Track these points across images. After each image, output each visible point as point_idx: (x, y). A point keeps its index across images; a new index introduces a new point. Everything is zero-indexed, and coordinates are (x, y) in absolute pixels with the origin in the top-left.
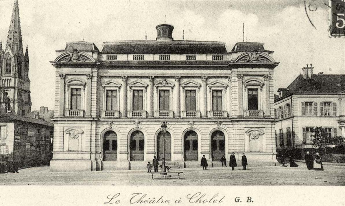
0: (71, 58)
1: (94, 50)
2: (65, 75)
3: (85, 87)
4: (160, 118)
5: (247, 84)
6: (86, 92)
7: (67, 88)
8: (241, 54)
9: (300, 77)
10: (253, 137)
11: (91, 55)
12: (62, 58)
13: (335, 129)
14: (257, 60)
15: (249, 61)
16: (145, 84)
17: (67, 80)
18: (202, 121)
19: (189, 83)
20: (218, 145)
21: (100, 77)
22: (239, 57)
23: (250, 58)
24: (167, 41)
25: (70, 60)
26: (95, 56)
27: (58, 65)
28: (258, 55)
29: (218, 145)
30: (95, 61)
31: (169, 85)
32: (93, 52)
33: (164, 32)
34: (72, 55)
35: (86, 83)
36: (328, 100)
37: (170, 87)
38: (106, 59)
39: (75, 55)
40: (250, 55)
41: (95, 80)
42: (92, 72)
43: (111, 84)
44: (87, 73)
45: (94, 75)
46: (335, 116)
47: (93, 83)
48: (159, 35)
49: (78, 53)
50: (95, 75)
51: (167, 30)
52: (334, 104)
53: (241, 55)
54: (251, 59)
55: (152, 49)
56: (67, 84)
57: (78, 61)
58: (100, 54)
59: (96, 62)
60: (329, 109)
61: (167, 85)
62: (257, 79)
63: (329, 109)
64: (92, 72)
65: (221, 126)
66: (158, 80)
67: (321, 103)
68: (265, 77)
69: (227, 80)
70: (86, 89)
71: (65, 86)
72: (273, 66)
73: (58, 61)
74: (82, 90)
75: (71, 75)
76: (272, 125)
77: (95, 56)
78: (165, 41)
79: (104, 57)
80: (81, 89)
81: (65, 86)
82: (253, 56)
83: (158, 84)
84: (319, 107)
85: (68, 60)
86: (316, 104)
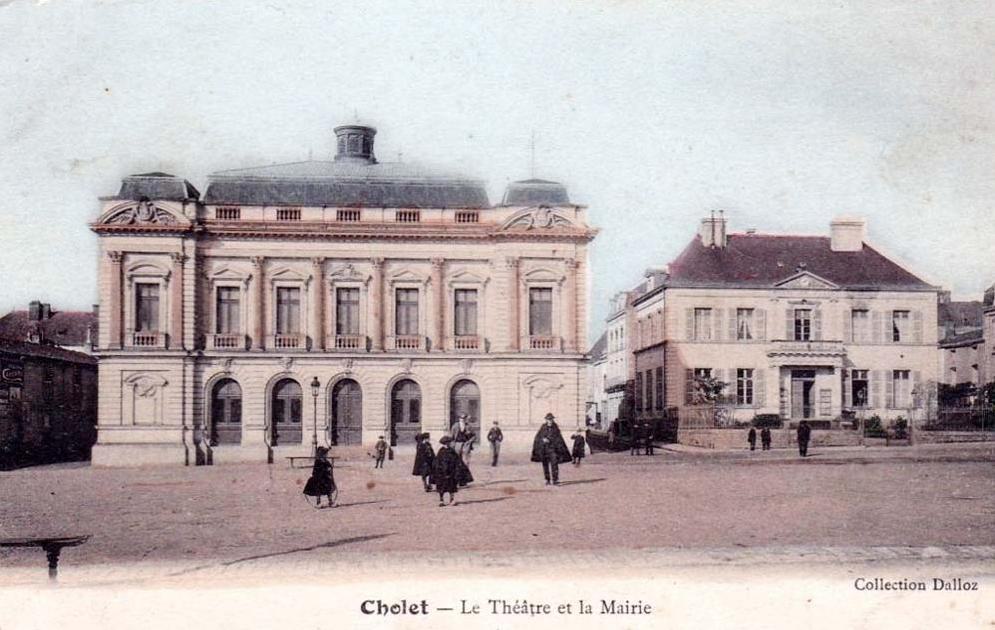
0: (135, 216)
1: (186, 196)
2: (120, 253)
3: (167, 280)
4: (336, 352)
5: (527, 277)
6: (170, 291)
7: (127, 282)
8: (514, 212)
9: (697, 242)
10: (537, 394)
11: (181, 211)
12: (114, 217)
13: (761, 372)
14: (548, 227)
15: (531, 228)
16: (303, 274)
17: (126, 263)
18: (428, 359)
19: (403, 273)
20: (406, 408)
21: (201, 259)
22: (510, 218)
23: (533, 220)
24: (357, 170)
25: (133, 222)
26: (191, 209)
27: (103, 229)
28: (550, 216)
29: (406, 408)
30: (189, 224)
31: (359, 277)
32: (185, 202)
33: (354, 143)
34: (138, 208)
35: (170, 273)
36: (748, 303)
37: (361, 281)
38: (214, 217)
39: (144, 210)
40: (533, 213)
41: (190, 265)
42: (184, 248)
43: (227, 273)
44: (173, 250)
45: (188, 254)
46: (762, 340)
47: (185, 271)
48: (341, 151)
49: (151, 205)
50: (191, 253)
51: (361, 141)
52: (762, 313)
53: (515, 215)
54: (536, 225)
55: (316, 194)
56: (127, 274)
57: (151, 223)
58: (200, 206)
59: (192, 227)
60: (752, 323)
61: (353, 277)
62: (548, 266)
63: (752, 323)
64: (184, 248)
65: (472, 370)
66: (335, 264)
67: (731, 310)
68: (567, 262)
69: (487, 266)
70: (170, 285)
71: (122, 279)
72: (584, 239)
73: (106, 223)
74: (161, 287)
75: (134, 253)
76: (579, 368)
77: (191, 209)
78: (357, 170)
79: (211, 213)
80: (158, 285)
81: (122, 279)
82: (539, 218)
83: (333, 275)
84: (726, 317)
85: (128, 221)
86: (720, 312)
